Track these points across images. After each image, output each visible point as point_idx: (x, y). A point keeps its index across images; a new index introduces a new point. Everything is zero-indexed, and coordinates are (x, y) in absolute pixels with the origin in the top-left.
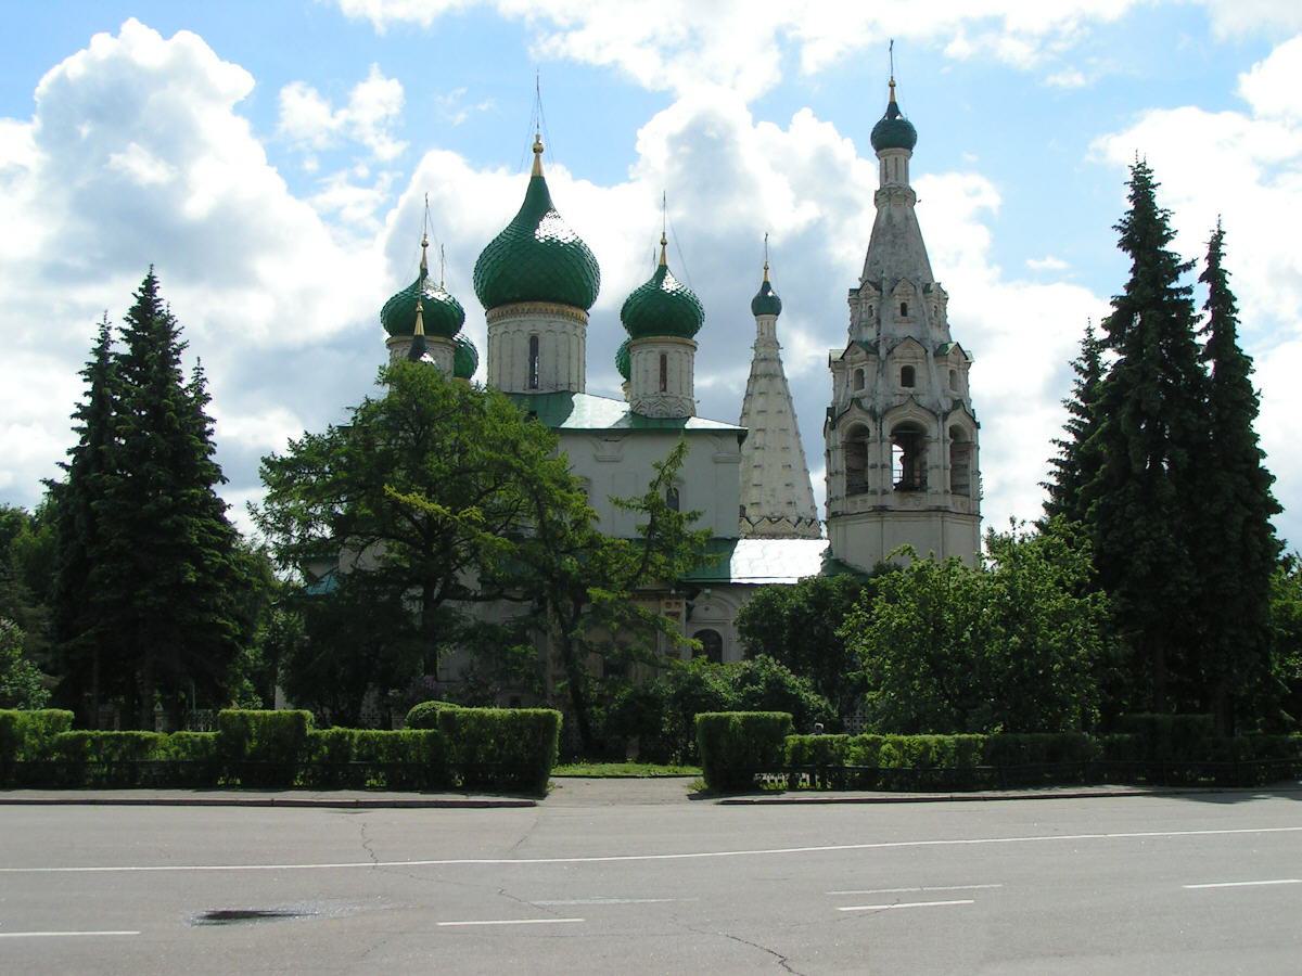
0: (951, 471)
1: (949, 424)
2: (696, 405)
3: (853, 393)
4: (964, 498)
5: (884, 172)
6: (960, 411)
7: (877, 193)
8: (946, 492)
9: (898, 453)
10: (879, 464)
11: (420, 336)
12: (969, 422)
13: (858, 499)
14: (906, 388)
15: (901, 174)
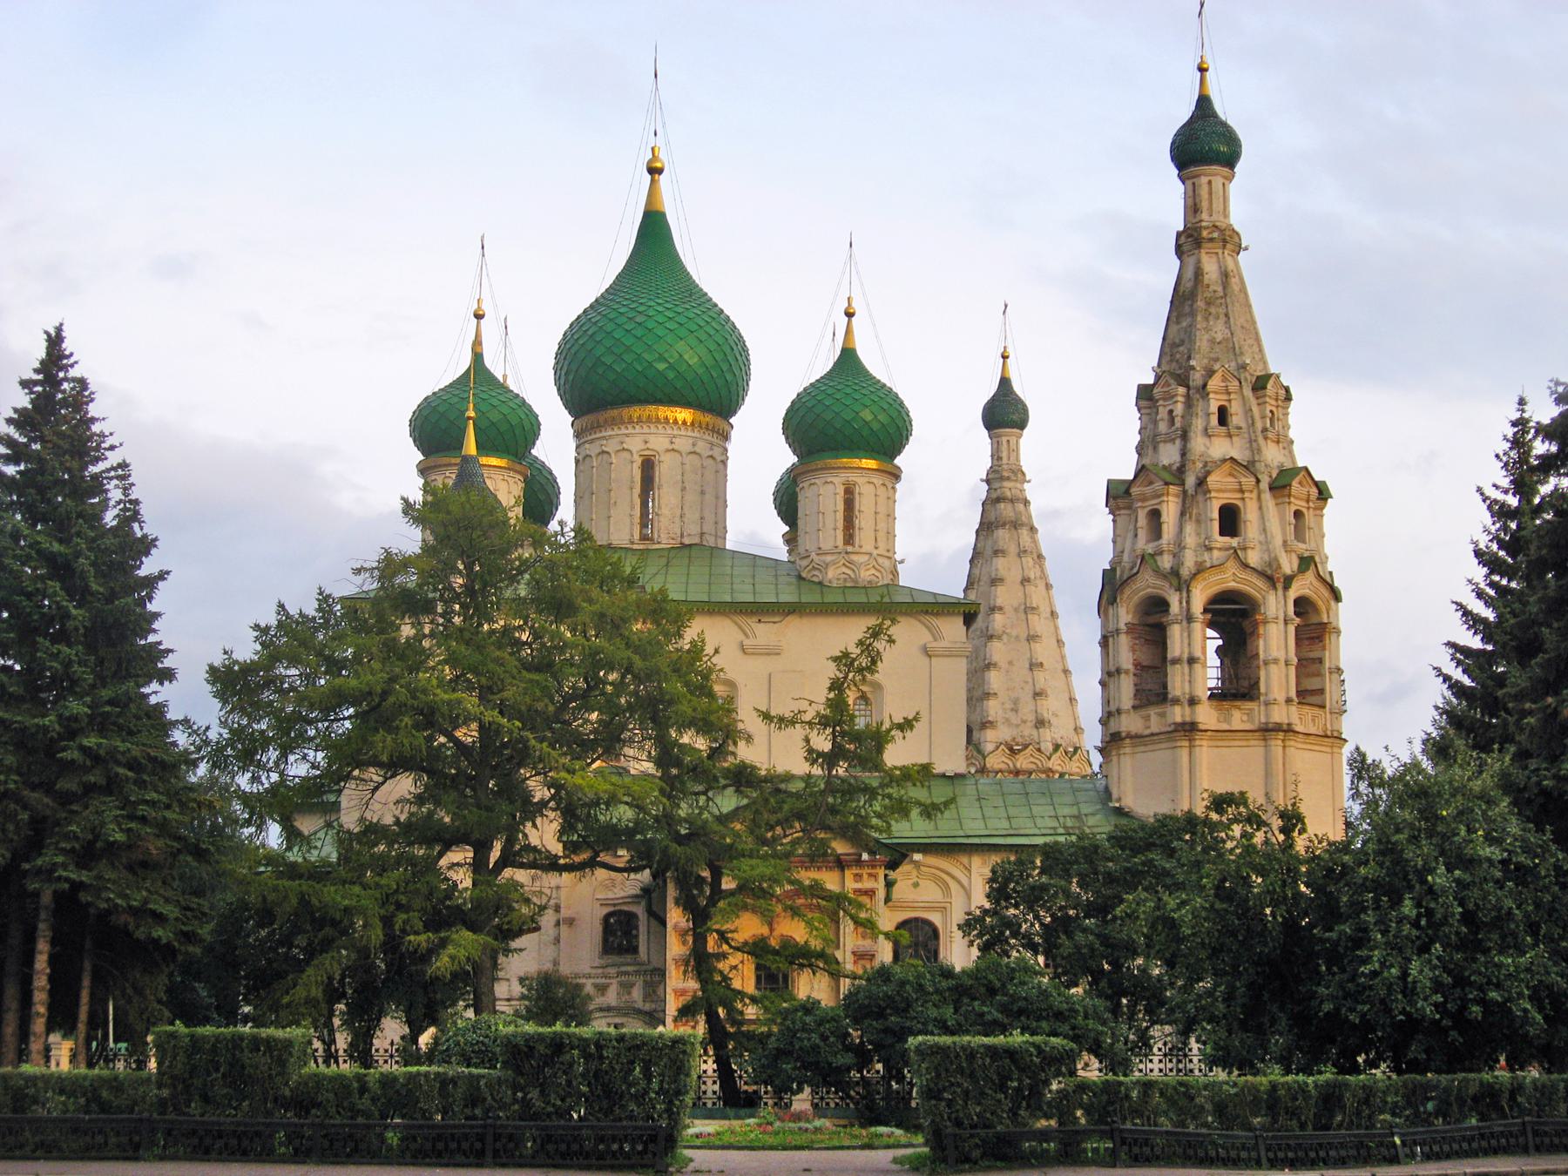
0: (1297, 668)
1: (1293, 594)
2: (899, 567)
3: (1143, 544)
4: (1317, 711)
5: (1190, 201)
6: (1310, 575)
7: (1179, 235)
8: (1289, 701)
9: (1213, 640)
10: (1185, 656)
11: (472, 457)
12: (1326, 593)
13: (1153, 712)
14: (1227, 539)
15: (1217, 205)
